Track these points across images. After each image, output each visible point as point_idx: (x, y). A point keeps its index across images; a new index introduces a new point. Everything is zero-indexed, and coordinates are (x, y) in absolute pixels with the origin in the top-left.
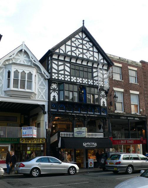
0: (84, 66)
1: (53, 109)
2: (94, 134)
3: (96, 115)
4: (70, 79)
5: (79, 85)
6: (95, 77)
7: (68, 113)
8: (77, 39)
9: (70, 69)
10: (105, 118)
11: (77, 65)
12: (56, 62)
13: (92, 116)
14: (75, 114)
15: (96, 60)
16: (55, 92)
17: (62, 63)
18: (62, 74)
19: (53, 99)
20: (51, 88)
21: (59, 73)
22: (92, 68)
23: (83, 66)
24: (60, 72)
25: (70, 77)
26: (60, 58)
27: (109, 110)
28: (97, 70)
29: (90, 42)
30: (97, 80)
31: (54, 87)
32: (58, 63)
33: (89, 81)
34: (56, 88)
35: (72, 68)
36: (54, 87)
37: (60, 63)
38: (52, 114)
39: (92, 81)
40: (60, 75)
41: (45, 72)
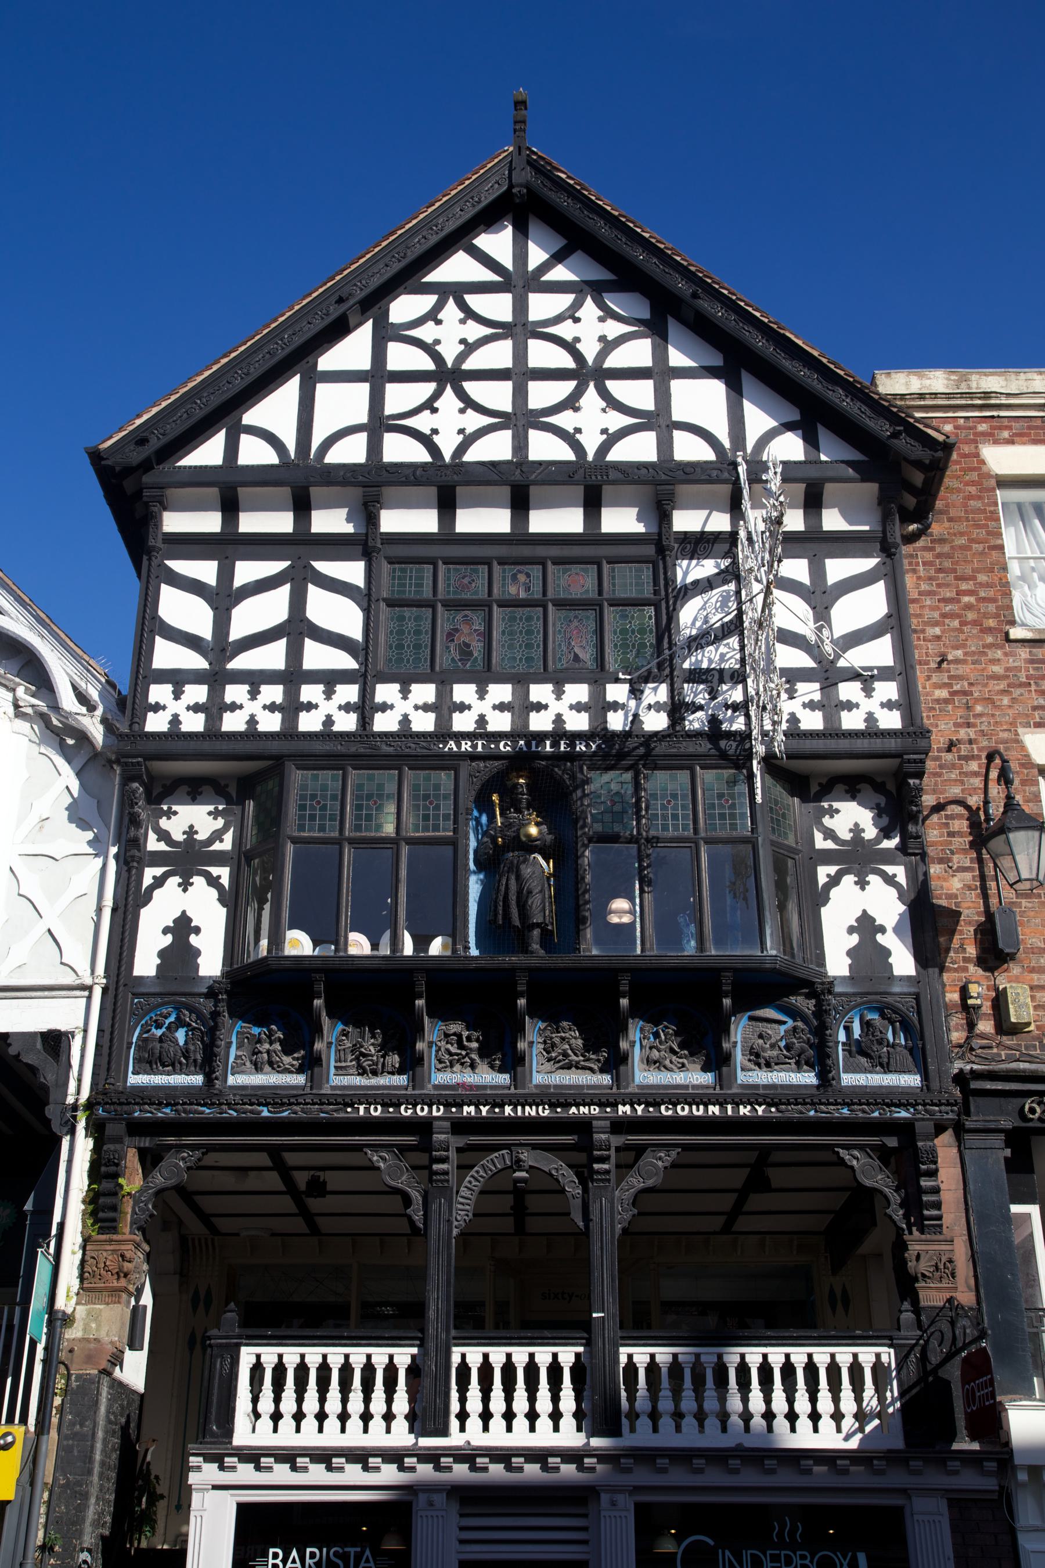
0: (555, 551)
1: (150, 1062)
2: (811, 1368)
3: (753, 1095)
4: (366, 708)
5: (473, 757)
6: (699, 641)
7: (348, 1099)
8: (457, 291)
9: (367, 611)
10: (905, 1130)
11: (526, 551)
12: (206, 571)
13: (744, 1111)
14: (437, 1112)
15: (704, 453)
16: (198, 881)
17: (866, 564)
18: (255, 680)
19: (162, 954)
20: (154, 844)
21: (231, 666)
22: (662, 550)
23: (541, 551)
24: (243, 662)
25: (367, 694)
26: (250, 523)
27: (971, 1026)
28: (735, 563)
29: (619, 286)
30: (738, 677)
31: (191, 831)
32: (818, 571)
33: (617, 692)
34: (217, 835)
35: (621, 594)
36: (191, 831)
37: (837, 569)
38: (136, 1128)
39: (658, 693)
40: (695, 693)
41: (82, 685)
